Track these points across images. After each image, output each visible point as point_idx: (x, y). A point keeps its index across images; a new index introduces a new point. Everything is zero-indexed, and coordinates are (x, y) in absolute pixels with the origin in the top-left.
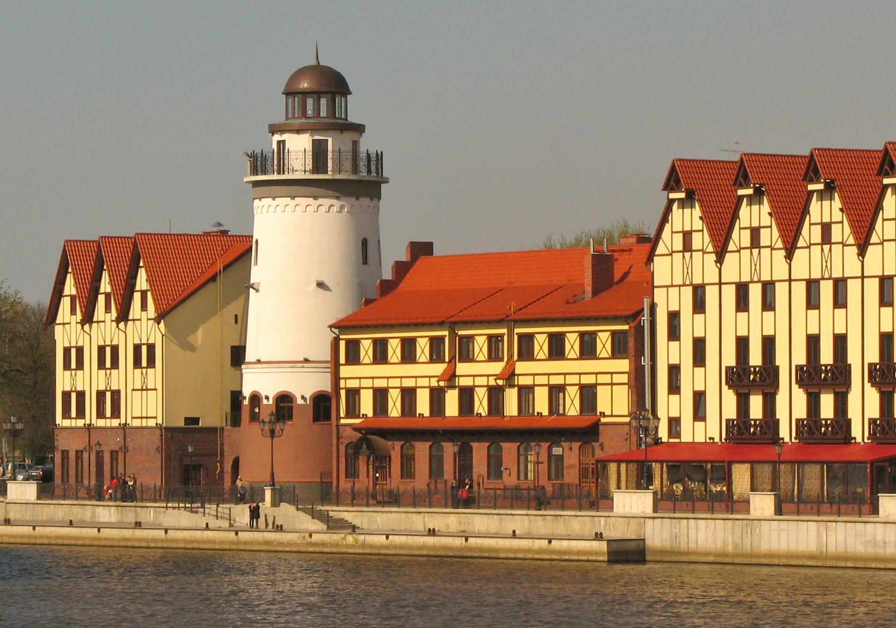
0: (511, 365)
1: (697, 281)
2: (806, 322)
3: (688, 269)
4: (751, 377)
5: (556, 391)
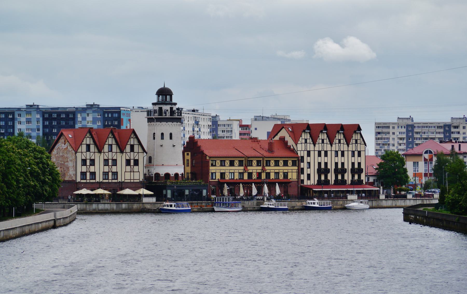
0: (263, 167)
1: (308, 150)
2: (335, 160)
3: (306, 147)
4: (323, 171)
5: (277, 174)
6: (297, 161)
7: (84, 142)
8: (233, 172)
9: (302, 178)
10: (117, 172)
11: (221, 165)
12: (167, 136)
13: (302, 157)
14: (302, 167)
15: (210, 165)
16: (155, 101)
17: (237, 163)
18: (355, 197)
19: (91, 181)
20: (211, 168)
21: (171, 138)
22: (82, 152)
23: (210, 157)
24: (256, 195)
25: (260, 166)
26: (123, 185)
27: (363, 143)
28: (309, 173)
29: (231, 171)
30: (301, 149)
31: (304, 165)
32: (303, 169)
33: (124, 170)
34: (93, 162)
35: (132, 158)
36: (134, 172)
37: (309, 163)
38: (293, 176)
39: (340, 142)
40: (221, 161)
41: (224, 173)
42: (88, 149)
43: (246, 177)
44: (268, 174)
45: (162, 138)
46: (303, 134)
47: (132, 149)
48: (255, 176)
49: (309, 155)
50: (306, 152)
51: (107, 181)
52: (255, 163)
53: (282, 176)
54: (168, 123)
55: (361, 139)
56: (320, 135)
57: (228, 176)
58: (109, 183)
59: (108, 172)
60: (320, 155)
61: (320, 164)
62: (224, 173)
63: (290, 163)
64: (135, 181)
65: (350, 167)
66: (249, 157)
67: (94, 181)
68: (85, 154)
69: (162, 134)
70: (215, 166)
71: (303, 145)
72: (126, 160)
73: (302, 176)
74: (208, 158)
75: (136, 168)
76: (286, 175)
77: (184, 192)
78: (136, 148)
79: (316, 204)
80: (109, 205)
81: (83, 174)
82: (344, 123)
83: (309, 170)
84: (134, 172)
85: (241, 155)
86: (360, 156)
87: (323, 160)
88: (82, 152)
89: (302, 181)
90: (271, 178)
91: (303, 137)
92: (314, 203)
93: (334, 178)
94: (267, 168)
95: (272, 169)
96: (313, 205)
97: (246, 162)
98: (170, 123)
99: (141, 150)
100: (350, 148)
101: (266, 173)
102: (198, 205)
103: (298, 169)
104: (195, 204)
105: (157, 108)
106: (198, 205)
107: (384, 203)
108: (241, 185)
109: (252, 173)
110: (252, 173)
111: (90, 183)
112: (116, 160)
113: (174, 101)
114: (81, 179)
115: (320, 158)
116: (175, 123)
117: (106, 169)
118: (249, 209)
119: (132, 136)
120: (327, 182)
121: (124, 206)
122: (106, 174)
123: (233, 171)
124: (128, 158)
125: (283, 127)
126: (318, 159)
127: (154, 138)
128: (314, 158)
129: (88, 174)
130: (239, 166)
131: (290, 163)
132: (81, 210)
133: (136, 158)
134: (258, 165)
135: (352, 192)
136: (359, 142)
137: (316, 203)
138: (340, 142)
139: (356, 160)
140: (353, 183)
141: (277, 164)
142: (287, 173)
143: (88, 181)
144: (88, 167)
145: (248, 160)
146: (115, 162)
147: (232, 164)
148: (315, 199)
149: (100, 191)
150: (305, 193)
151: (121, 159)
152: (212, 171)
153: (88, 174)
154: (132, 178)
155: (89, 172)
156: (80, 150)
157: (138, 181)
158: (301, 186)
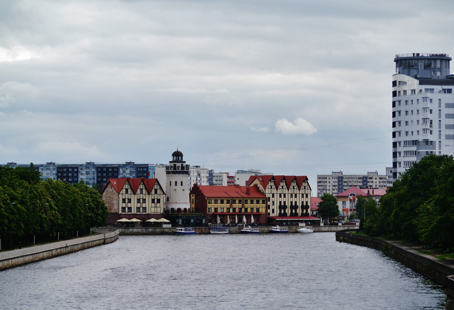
3: (271, 191)
4: (282, 207)
5: (252, 209)
6: (266, 200)
7: (124, 187)
8: (223, 207)
9: (269, 212)
10: (146, 207)
11: (215, 203)
12: (179, 184)
13: (269, 198)
14: (269, 204)
16: (171, 160)
17: (225, 201)
18: (304, 224)
21: (182, 185)
23: (208, 198)
24: (238, 223)
26: (150, 216)
30: (268, 192)
32: (269, 206)
33: (150, 206)
34: (130, 201)
35: (156, 198)
37: (273, 202)
38: (262, 210)
39: (294, 188)
40: (215, 200)
41: (217, 208)
42: (127, 192)
43: (231, 211)
44: (246, 209)
45: (176, 185)
46: (270, 183)
47: (156, 192)
48: (237, 210)
49: (273, 196)
50: (271, 195)
51: (139, 213)
52: (237, 201)
58: (140, 214)
59: (140, 207)
60: (280, 196)
61: (280, 202)
62: (217, 208)
65: (301, 205)
68: (124, 195)
69: (176, 182)
70: (211, 203)
73: (269, 210)
74: (206, 198)
75: (158, 205)
76: (258, 210)
77: (190, 221)
78: (159, 191)
81: (123, 209)
82: (297, 175)
85: (228, 196)
87: (283, 199)
89: (269, 214)
93: (290, 212)
94: (245, 205)
95: (248, 206)
99: (161, 193)
100: (301, 192)
101: (245, 208)
103: (266, 206)
105: (172, 164)
107: (323, 229)
109: (235, 208)
110: (235, 208)
111: (128, 214)
112: (145, 199)
113: (184, 160)
116: (185, 175)
117: (139, 205)
120: (285, 215)
121: (150, 230)
122: (138, 209)
124: (153, 198)
125: (256, 178)
126: (279, 199)
127: (171, 185)
128: (277, 198)
129: (127, 208)
130: (227, 203)
134: (239, 203)
135: (302, 222)
136: (306, 187)
137: (278, 228)
138: (294, 188)
139: (305, 200)
141: (252, 202)
146: (144, 201)
147: (222, 202)
149: (134, 220)
150: (271, 221)
151: (149, 199)
153: (127, 208)
156: (121, 193)
158: (268, 217)
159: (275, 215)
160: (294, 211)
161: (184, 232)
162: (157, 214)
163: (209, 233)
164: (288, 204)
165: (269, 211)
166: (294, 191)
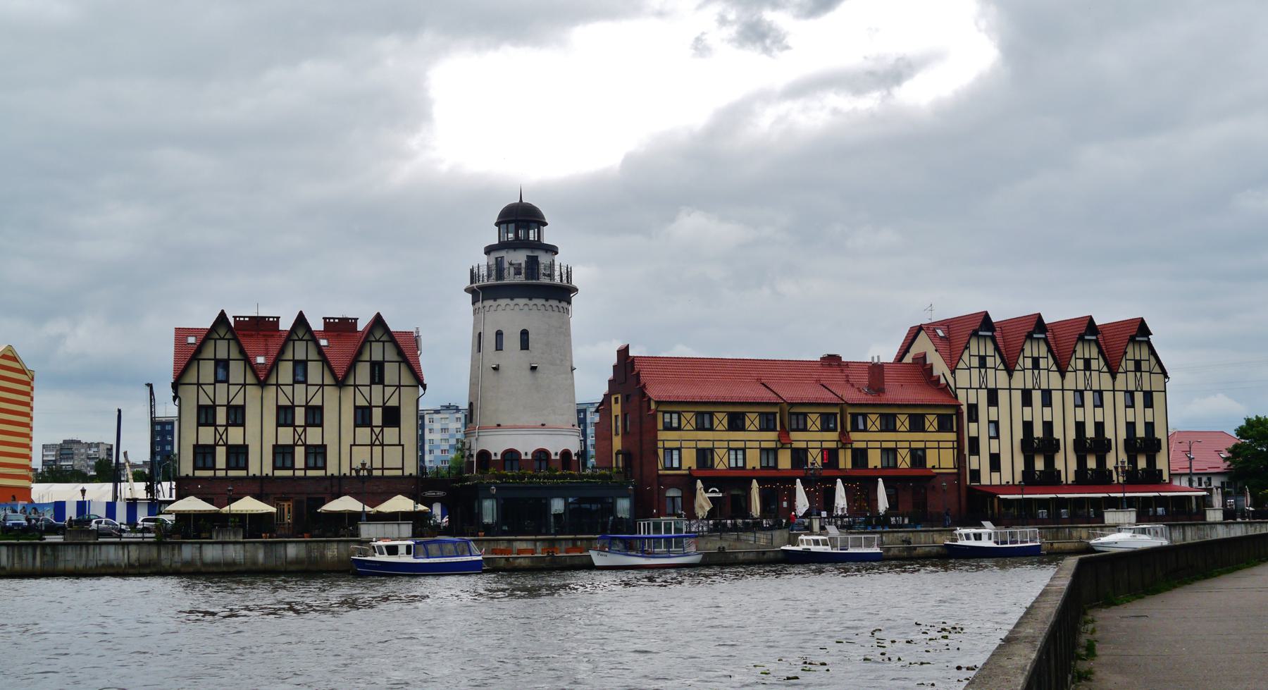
1: (991, 385)
4: (1038, 445)
5: (890, 453)
6: (952, 417)
8: (746, 448)
9: (974, 466)
10: (324, 447)
11: (700, 427)
12: (512, 341)
13: (973, 408)
14: (973, 433)
15: (660, 426)
17: (752, 420)
18: (1129, 516)
19: (232, 473)
20: (662, 435)
21: (525, 345)
22: (199, 385)
23: (658, 403)
24: (807, 514)
25: (835, 430)
26: (338, 486)
27: (1157, 369)
28: (995, 450)
29: (732, 445)
30: (967, 384)
31: (979, 429)
32: (974, 442)
33: (347, 440)
34: (237, 415)
35: (377, 401)
36: (382, 445)
37: (996, 423)
38: (941, 459)
39: (1087, 366)
40: (699, 415)
41: (712, 450)
42: (221, 376)
43: (785, 461)
44: (860, 456)
45: (499, 347)
46: (973, 344)
47: (377, 374)
49: (993, 398)
50: (983, 394)
51: (289, 473)
52: (814, 421)
53: (908, 459)
54: (517, 301)
55: (1152, 359)
56: (1027, 347)
57: (725, 460)
58: (293, 478)
60: (1027, 399)
61: (1028, 426)
62: (712, 450)
63: (931, 421)
64: (387, 473)
65: (1122, 434)
66: (792, 405)
67: (242, 473)
68: (210, 389)
69: (499, 334)
70: (679, 429)
71: (975, 372)
72: (356, 408)
74: (653, 406)
75: (390, 434)
76: (918, 457)
77: (547, 506)
78: (391, 372)
79: (985, 537)
80: (238, 547)
83: (994, 442)
84: (382, 445)
85: (766, 395)
86: (1151, 406)
88: (199, 385)
89: (976, 474)
90: (871, 465)
91: (974, 350)
92: (978, 537)
93: (1073, 465)
94: (854, 436)
95: (872, 439)
96: (973, 543)
97: (782, 417)
98: (522, 301)
99: (407, 379)
102: (574, 545)
103: (960, 440)
104: (564, 546)
106: (574, 545)
108: (755, 484)
109: (806, 450)
110: (806, 450)
111: (226, 478)
112: (320, 409)
114: (195, 468)
115: (1027, 410)
116: (540, 302)
117: (286, 436)
118: (741, 557)
119: (378, 334)
120: (1051, 478)
121: (292, 551)
122: (283, 454)
123: (741, 445)
124: (361, 402)
126: (1021, 414)
129: (221, 453)
131: (931, 421)
132: (141, 565)
133: (393, 402)
134: (825, 428)
136: (1144, 366)
137: (986, 535)
138: (1087, 366)
139: (1140, 416)
140: (1133, 478)
141: (888, 424)
142: (924, 450)
143: (221, 474)
144: (221, 430)
145: (791, 414)
146: (315, 416)
147: (736, 423)
148: (988, 524)
149: (248, 505)
150: (978, 504)
151: (339, 408)
152: (668, 445)
153: (300, 452)
154: (377, 464)
155: (226, 444)
156: (191, 377)
157: (399, 473)
158: (970, 488)
159: (1006, 476)
160: (1091, 463)
161: (410, 559)
162: (383, 477)
163: (590, 567)
164: (1065, 434)
165: (974, 462)
166: (1088, 380)
